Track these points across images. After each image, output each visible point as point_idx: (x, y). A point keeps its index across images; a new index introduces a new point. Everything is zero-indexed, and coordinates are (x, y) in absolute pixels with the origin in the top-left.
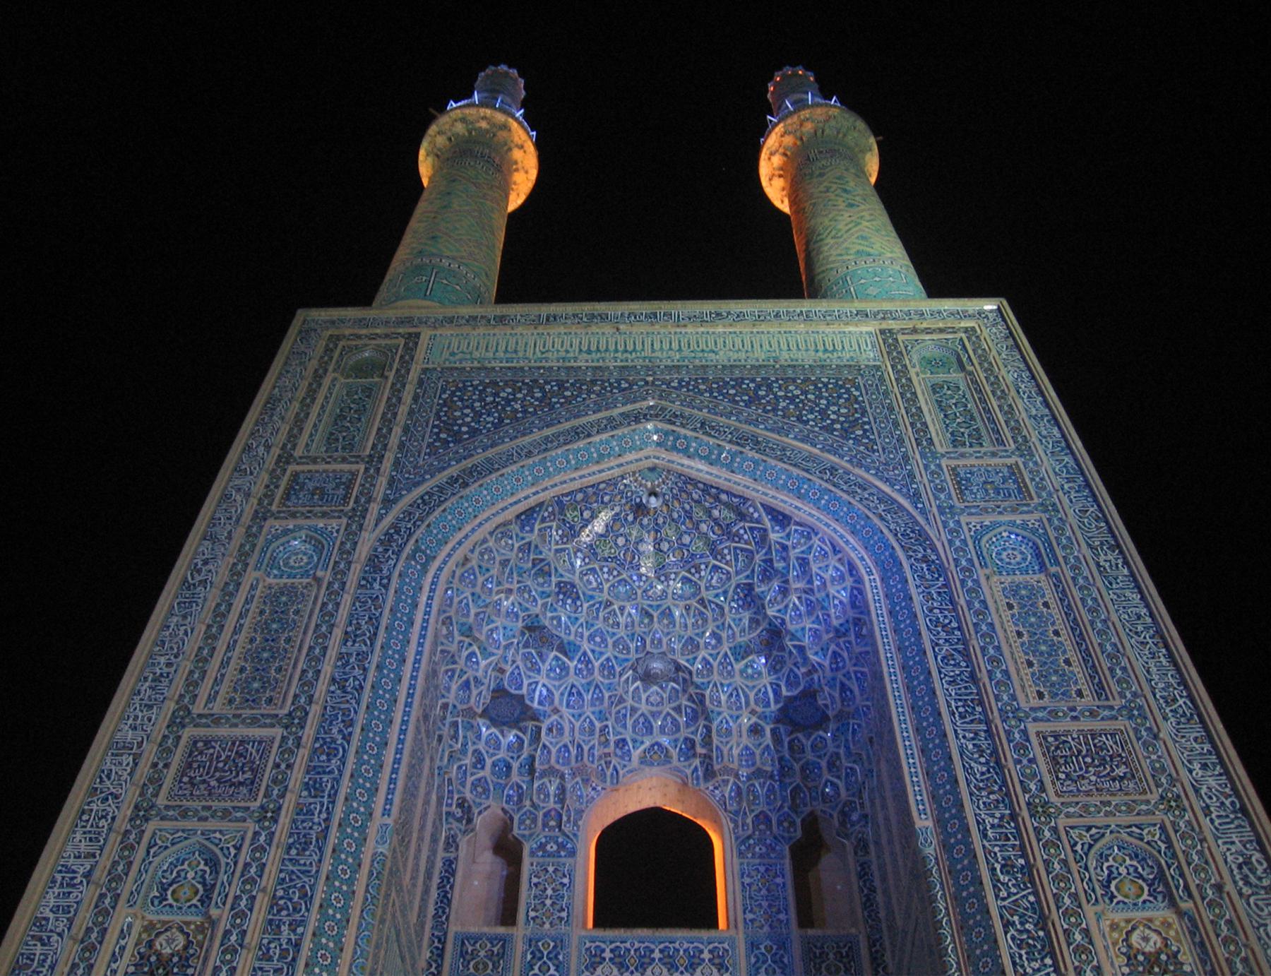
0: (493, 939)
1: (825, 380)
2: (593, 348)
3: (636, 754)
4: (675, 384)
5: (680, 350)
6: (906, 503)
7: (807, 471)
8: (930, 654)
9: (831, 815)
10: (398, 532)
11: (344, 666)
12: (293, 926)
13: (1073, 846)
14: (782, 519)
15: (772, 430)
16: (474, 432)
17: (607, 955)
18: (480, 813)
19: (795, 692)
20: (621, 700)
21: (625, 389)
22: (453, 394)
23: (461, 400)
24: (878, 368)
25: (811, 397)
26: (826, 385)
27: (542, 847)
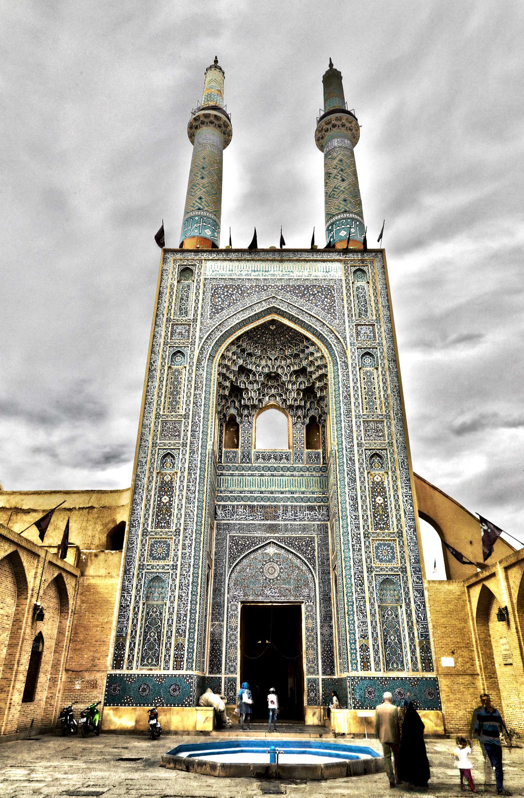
0: (235, 452)
1: (325, 286)
2: (256, 270)
4: (280, 288)
5: (282, 271)
6: (342, 340)
7: (316, 326)
8: (341, 395)
10: (204, 349)
11: (196, 397)
12: (195, 474)
13: (365, 455)
14: (308, 339)
15: (307, 309)
16: (222, 309)
17: (261, 456)
19: (309, 385)
20: (264, 383)
21: (265, 290)
22: (215, 292)
23: (217, 294)
24: (341, 280)
25: (320, 294)
26: (325, 288)
27: (244, 425)
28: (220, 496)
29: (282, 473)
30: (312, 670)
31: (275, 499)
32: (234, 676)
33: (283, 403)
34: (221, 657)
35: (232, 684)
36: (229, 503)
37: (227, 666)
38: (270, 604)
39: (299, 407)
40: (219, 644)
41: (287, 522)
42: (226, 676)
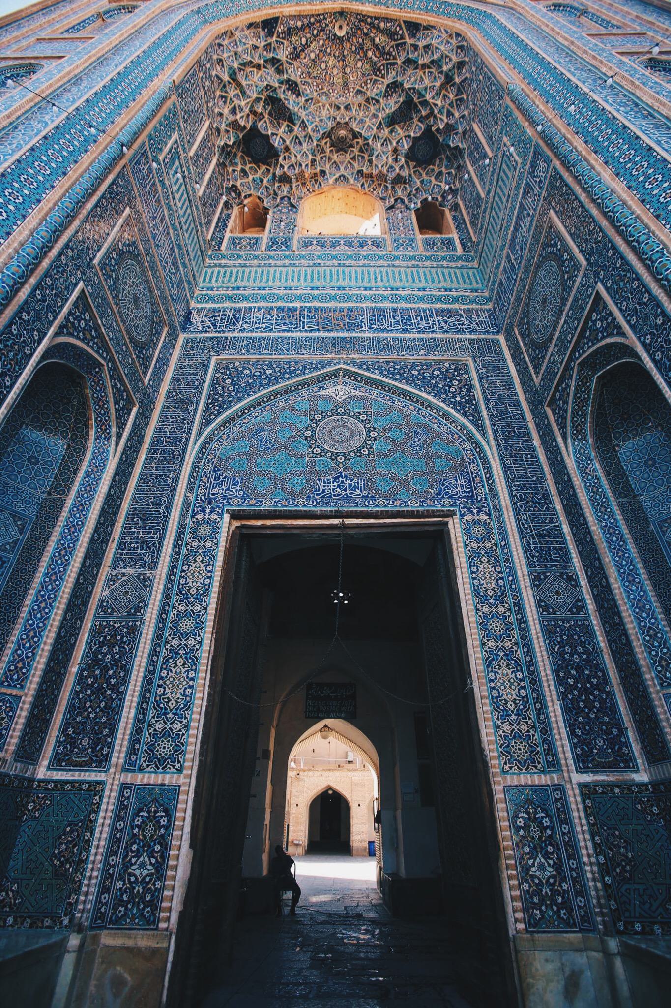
3: (331, 181)
9: (437, 199)
18: (245, 197)
19: (418, 135)
28: (207, 295)
29: (366, 262)
30: (521, 749)
31: (349, 298)
32: (168, 778)
33: (363, 185)
34: (121, 696)
35: (153, 818)
36: (227, 304)
37: (146, 736)
38: (336, 521)
39: (399, 180)
40: (121, 644)
41: (385, 335)
42: (129, 778)
